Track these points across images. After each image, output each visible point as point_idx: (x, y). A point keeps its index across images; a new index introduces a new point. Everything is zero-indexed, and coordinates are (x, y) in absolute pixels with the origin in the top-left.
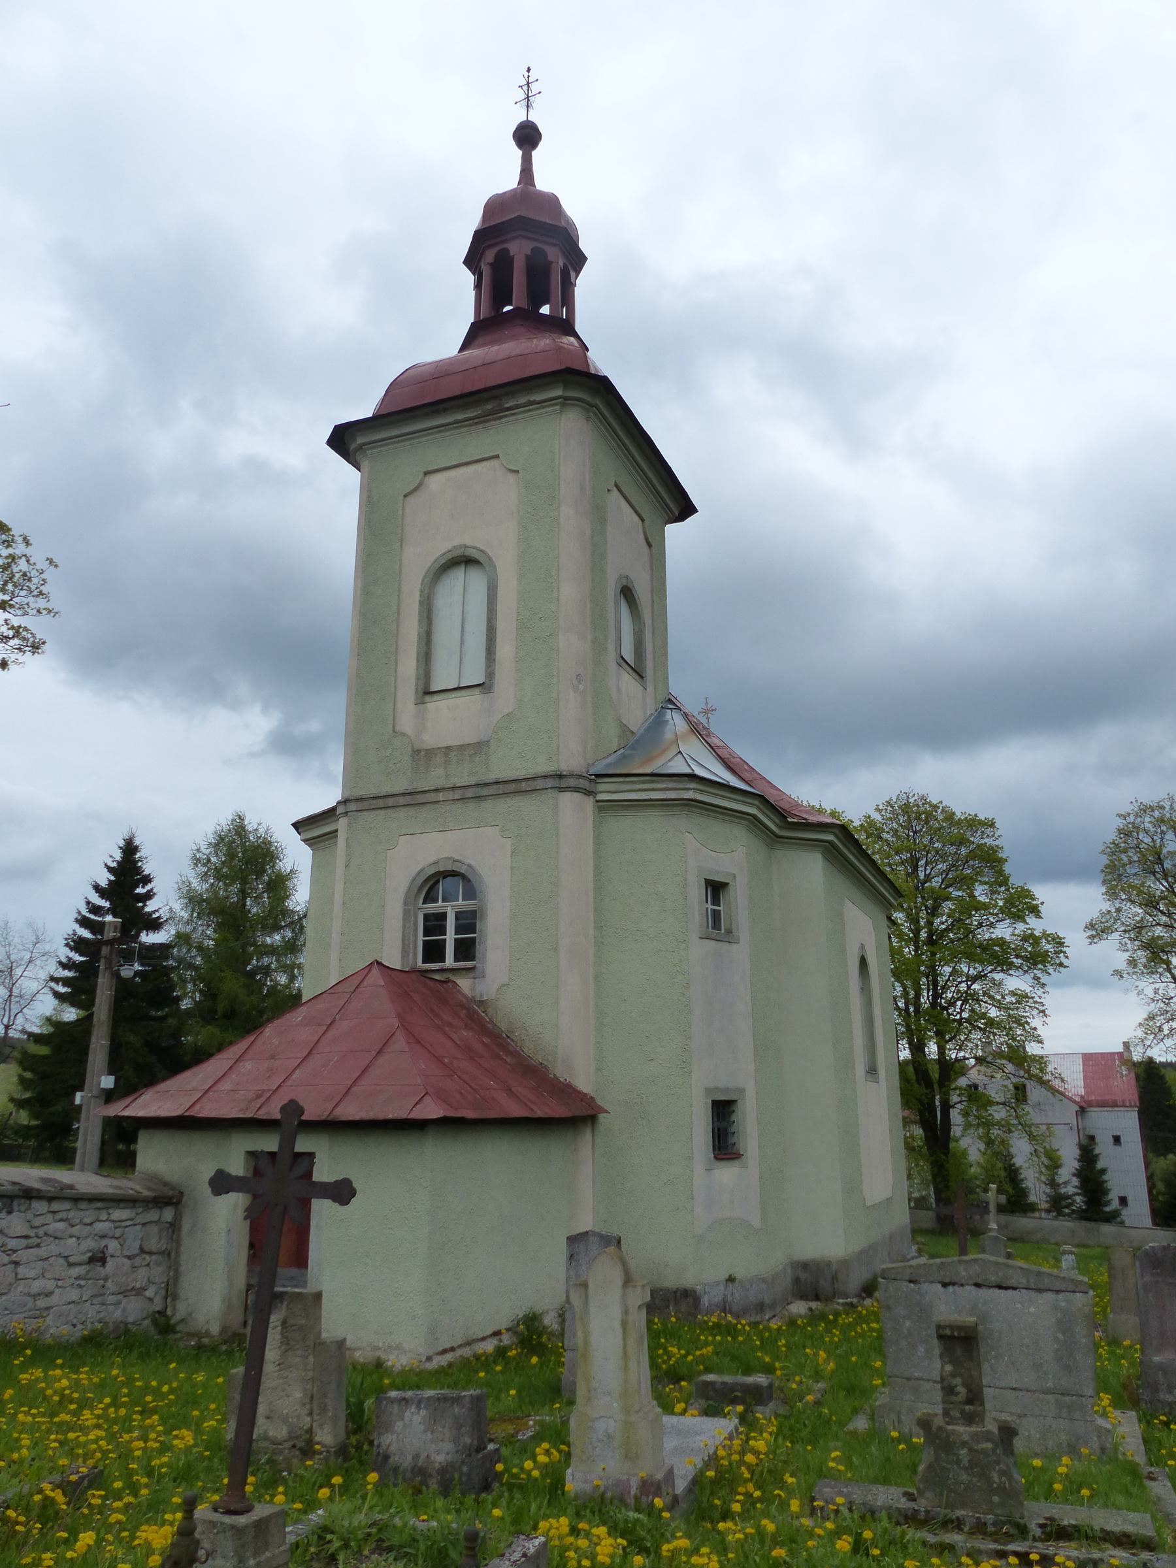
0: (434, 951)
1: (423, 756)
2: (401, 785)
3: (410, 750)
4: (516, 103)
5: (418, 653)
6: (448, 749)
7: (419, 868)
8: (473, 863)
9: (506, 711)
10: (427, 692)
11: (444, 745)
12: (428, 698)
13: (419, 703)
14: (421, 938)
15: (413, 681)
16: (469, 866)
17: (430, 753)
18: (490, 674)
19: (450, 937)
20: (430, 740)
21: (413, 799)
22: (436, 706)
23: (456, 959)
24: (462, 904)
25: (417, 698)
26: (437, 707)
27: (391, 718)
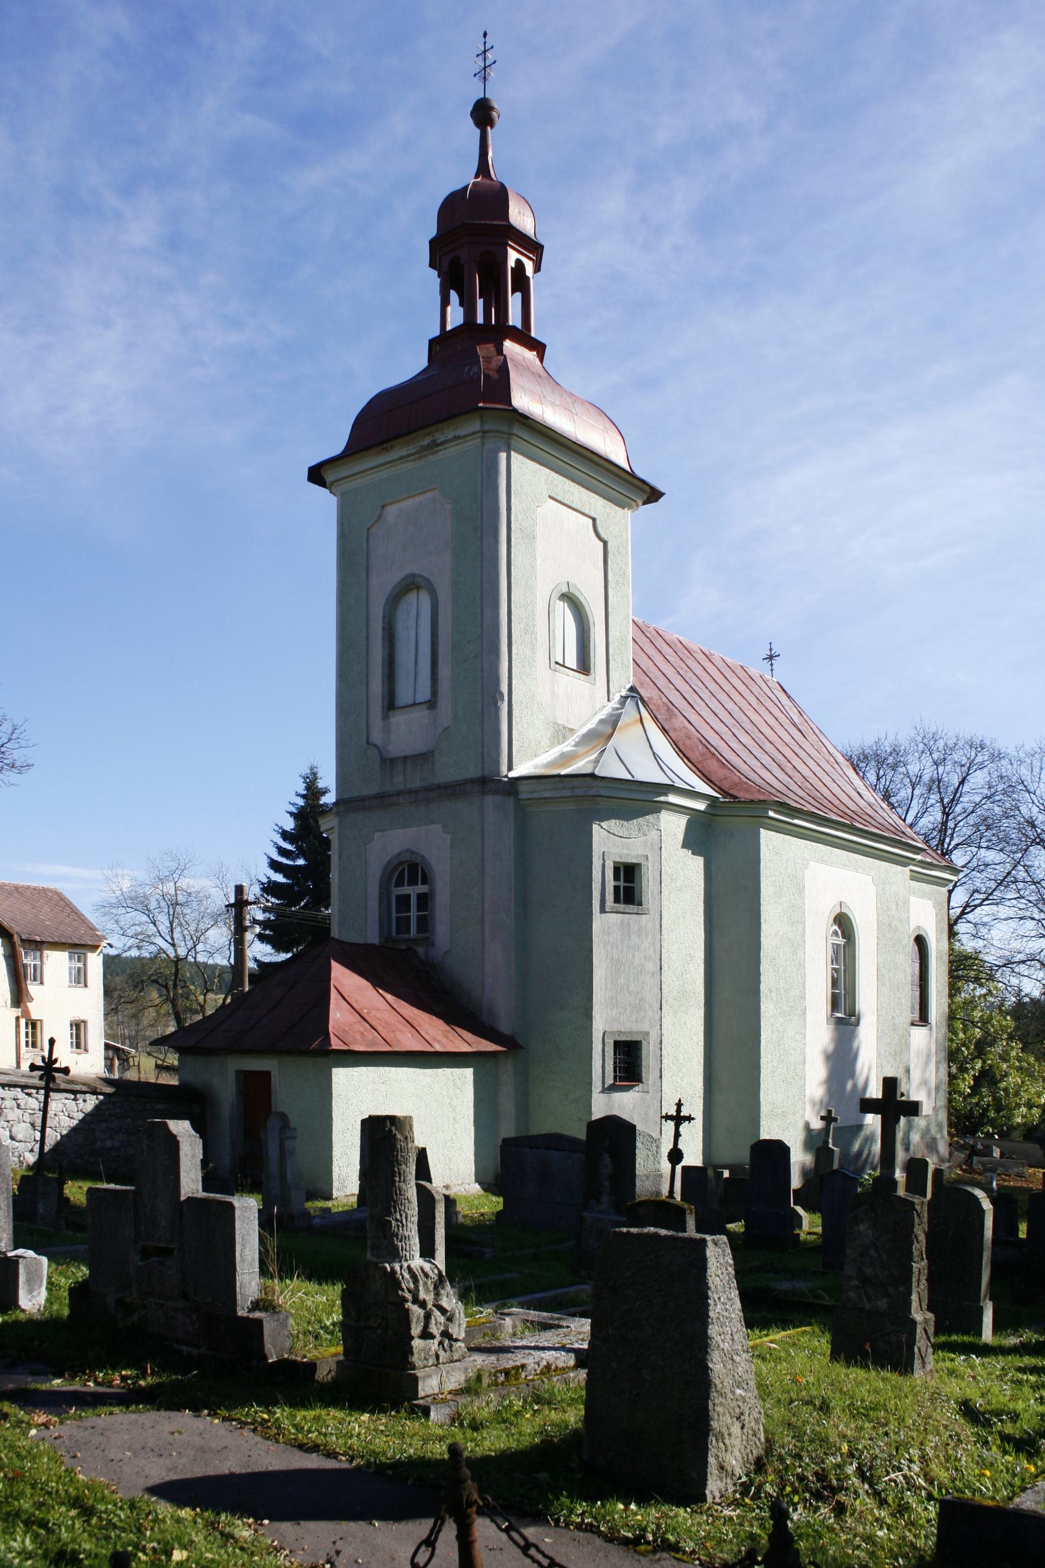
1: (389, 763)
2: (374, 789)
3: (379, 759)
4: (475, 75)
5: (383, 674)
6: (405, 758)
7: (389, 858)
8: (424, 854)
9: (446, 725)
11: (402, 754)
12: (391, 713)
13: (386, 717)
14: (394, 915)
15: (380, 699)
16: (423, 857)
17: (393, 761)
18: (434, 692)
19: (413, 914)
20: (395, 750)
21: (383, 800)
23: (418, 932)
24: (422, 889)
25: (383, 715)
26: (398, 719)
27: (365, 732)
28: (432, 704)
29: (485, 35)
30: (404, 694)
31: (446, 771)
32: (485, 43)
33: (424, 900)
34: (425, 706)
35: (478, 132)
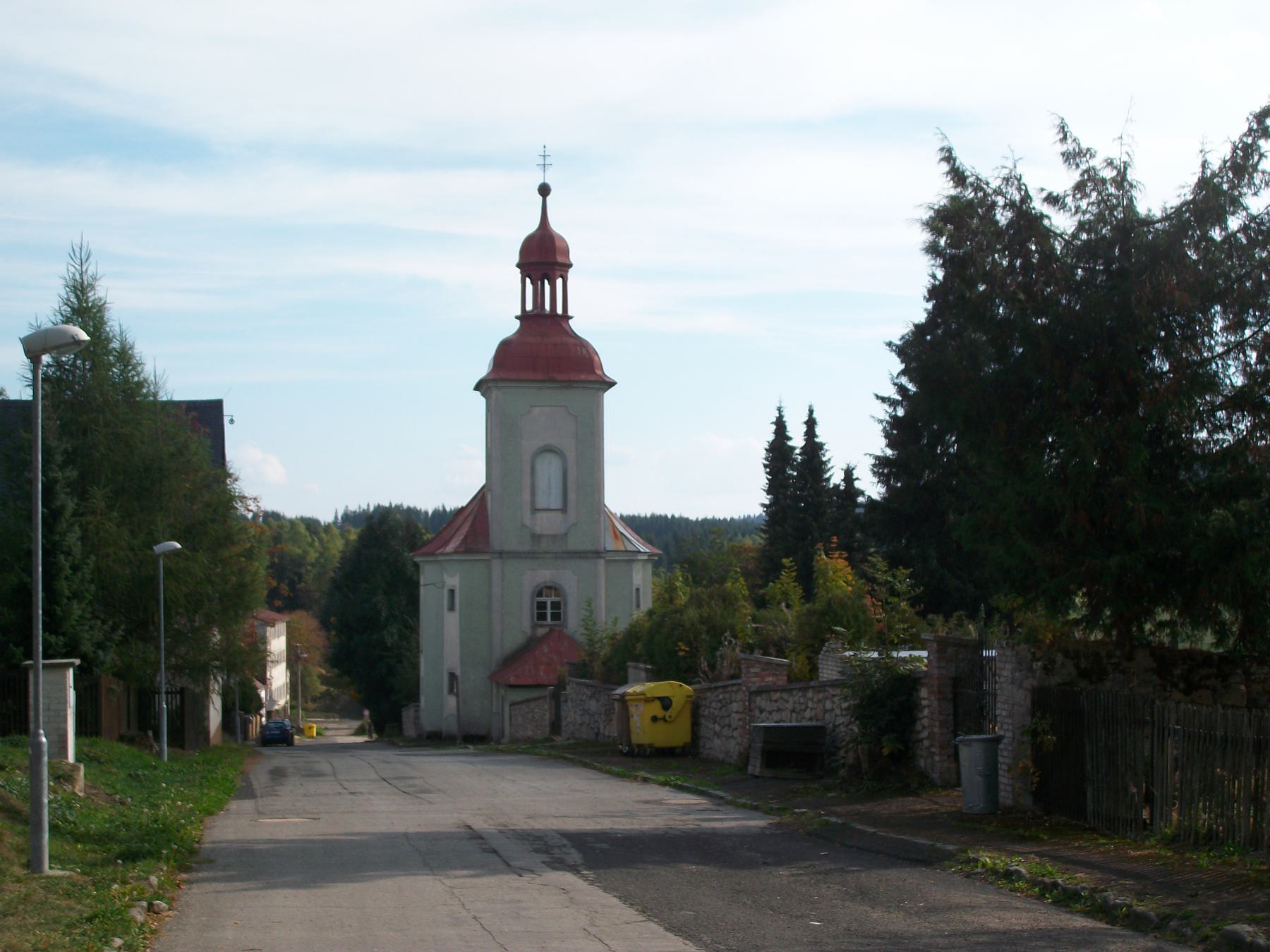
0: (542, 617)
1: (536, 538)
2: (527, 548)
6: (548, 535)
10: (535, 510)
19: (549, 611)
20: (538, 530)
21: (532, 555)
22: (539, 515)
24: (554, 599)
28: (564, 510)
29: (545, 147)
30: (541, 503)
31: (573, 544)
32: (545, 151)
33: (556, 605)
34: (559, 512)
35: (540, 198)
